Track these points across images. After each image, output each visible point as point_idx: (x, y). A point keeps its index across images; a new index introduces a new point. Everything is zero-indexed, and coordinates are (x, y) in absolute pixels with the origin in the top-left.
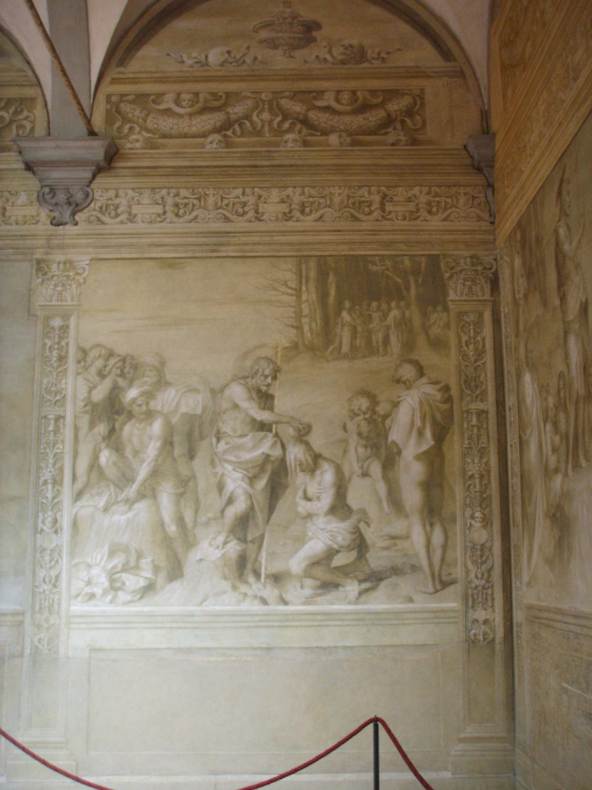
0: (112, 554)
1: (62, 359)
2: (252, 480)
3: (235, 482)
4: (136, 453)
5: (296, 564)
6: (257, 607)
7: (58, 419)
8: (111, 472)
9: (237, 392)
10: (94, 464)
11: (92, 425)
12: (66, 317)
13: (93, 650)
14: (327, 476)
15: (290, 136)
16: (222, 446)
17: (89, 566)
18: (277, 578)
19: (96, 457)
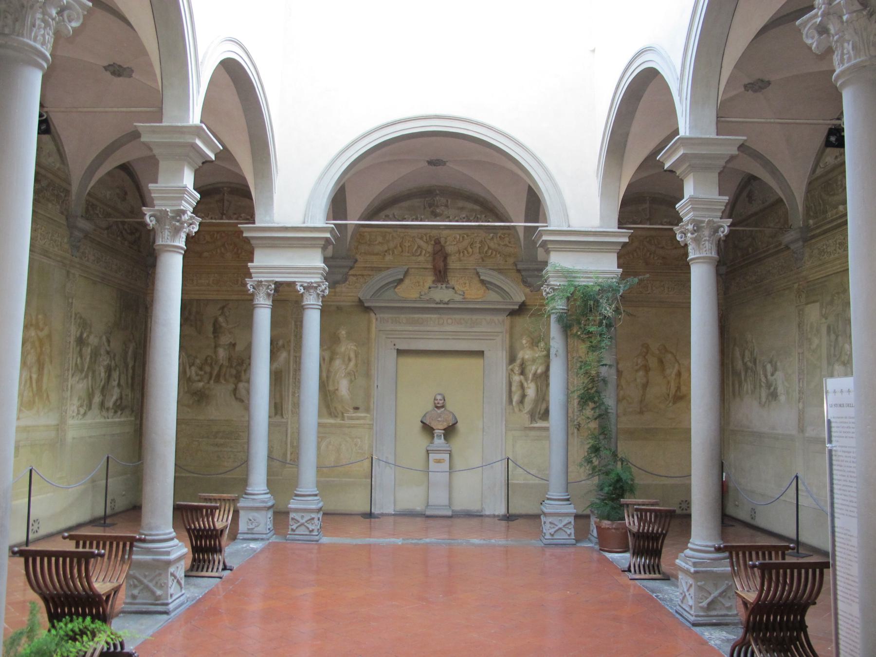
0: (78, 400)
1: (71, 317)
2: (105, 372)
3: (103, 374)
4: (85, 359)
5: (110, 404)
6: (103, 420)
7: (70, 342)
8: (80, 366)
9: (104, 338)
10: (76, 364)
11: (77, 346)
12: (72, 298)
13: (74, 438)
14: (118, 373)
15: (119, 238)
16: (101, 359)
17: (74, 405)
18: (108, 409)
19: (77, 361)
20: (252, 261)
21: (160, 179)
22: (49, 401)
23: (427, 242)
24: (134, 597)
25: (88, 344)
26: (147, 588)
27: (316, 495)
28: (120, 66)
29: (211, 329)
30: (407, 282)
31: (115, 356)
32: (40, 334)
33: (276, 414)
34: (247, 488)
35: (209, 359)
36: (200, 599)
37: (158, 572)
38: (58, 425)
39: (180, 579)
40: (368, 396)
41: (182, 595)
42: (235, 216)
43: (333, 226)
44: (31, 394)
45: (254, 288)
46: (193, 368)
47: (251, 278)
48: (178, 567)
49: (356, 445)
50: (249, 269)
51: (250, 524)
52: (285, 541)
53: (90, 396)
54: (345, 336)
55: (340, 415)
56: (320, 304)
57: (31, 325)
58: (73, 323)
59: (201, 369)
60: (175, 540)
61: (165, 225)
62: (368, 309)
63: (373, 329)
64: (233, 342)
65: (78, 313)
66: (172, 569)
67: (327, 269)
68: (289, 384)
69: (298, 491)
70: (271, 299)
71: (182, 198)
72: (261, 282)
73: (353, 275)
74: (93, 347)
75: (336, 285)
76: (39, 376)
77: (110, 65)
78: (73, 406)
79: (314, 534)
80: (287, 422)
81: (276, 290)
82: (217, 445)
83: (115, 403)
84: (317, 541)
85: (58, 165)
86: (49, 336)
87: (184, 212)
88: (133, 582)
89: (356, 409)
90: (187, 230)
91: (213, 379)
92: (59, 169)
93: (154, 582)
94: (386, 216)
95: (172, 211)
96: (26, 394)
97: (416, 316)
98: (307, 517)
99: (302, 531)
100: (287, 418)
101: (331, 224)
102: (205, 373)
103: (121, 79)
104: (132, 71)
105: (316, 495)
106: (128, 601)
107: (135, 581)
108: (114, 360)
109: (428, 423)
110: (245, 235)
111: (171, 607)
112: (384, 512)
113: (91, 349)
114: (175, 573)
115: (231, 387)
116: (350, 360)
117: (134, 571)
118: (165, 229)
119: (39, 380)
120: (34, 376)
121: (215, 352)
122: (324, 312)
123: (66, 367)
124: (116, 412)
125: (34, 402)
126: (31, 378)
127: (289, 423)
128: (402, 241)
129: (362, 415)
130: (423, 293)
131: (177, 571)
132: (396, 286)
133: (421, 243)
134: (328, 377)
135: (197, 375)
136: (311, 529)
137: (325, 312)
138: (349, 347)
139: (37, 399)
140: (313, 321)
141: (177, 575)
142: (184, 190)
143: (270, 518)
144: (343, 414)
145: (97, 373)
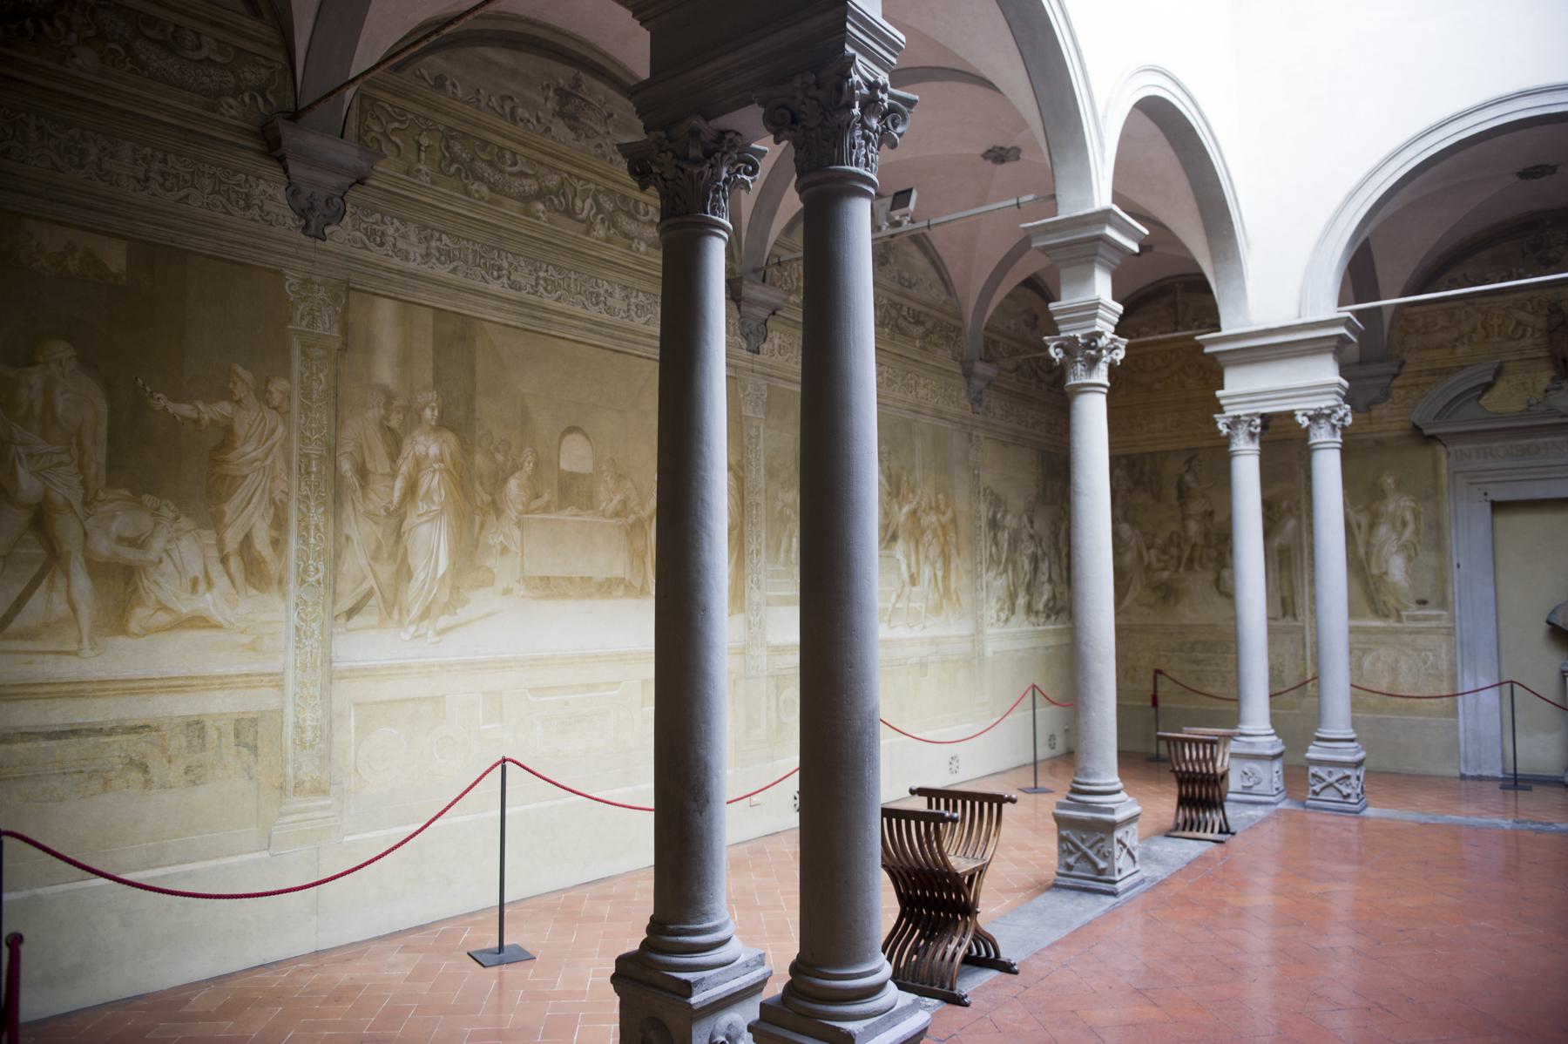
0: (997, 602)
1: (979, 493)
2: (1030, 563)
3: (1026, 562)
4: (1002, 548)
5: (1040, 606)
6: (1031, 628)
7: (980, 527)
8: (995, 558)
9: (1025, 518)
10: (991, 555)
11: (989, 532)
12: (979, 469)
14: (1047, 563)
16: (1023, 547)
18: (1037, 613)
20: (1222, 387)
21: (1064, 293)
22: (960, 604)
23: (1534, 313)
24: (1069, 867)
25: (1004, 527)
26: (1085, 856)
27: (1352, 740)
28: (1002, 149)
29: (1174, 493)
30: (1501, 385)
31: (1041, 540)
32: (941, 517)
33: (1285, 614)
34: (1240, 726)
35: (1175, 536)
36: (1162, 881)
37: (1099, 835)
38: (973, 635)
39: (1131, 849)
40: (1442, 581)
41: (1136, 872)
42: (1196, 323)
43: (1349, 314)
44: (936, 596)
45: (1228, 427)
46: (1153, 552)
47: (1223, 412)
48: (1127, 832)
49: (1425, 662)
50: (1217, 400)
51: (1246, 780)
52: (1302, 809)
53: (1013, 596)
54: (1393, 486)
55: (1394, 613)
56: (1340, 440)
57: (931, 508)
58: (982, 501)
59: (1164, 551)
60: (1122, 793)
61: (1076, 357)
62: (1433, 439)
63: (1444, 471)
64: (1210, 509)
65: (988, 487)
66: (1118, 834)
67: (1346, 384)
68: (1302, 569)
69: (1325, 733)
70: (1257, 441)
71: (1095, 316)
72: (1239, 417)
73: (1399, 387)
74: (1011, 531)
75: (1371, 407)
76: (945, 572)
77: (989, 151)
78: (991, 610)
79: (1351, 800)
80: (1304, 627)
81: (1264, 426)
82: (1197, 662)
83: (1046, 605)
84: (1357, 812)
85: (943, 298)
86: (954, 521)
87: (1100, 335)
88: (1068, 847)
89: (1422, 603)
90: (1107, 359)
91: (1183, 565)
92: (945, 302)
93: (1095, 850)
94: (1450, 281)
95: (1084, 336)
96: (930, 596)
97: (1524, 442)
98: (1338, 774)
99: (1330, 795)
100: (1304, 620)
101: (1346, 312)
102: (1171, 557)
103: (1005, 166)
104: (1019, 150)
105: (1352, 740)
106: (1063, 871)
107: (1070, 845)
108: (1041, 546)
109: (1560, 624)
110: (1207, 350)
111: (1120, 886)
112: (1485, 773)
113: (1009, 533)
114: (1124, 840)
115: (1211, 576)
116: (1404, 524)
117: (1068, 832)
118: (1076, 362)
119: (946, 578)
120: (940, 573)
121: (1184, 527)
122: (1347, 453)
123: (978, 560)
124: (1048, 617)
125: (941, 606)
126: (935, 575)
127: (1307, 627)
128: (1486, 319)
129: (1434, 612)
130: (1534, 401)
131: (1127, 837)
132: (1480, 397)
133: (1523, 316)
134: (1368, 554)
135: (1159, 560)
136: (1345, 793)
137: (1349, 453)
138: (1402, 504)
139: (945, 603)
140: (1328, 469)
141: (1127, 843)
142: (1096, 305)
143: (1277, 772)
144: (1398, 611)
145: (1019, 565)
